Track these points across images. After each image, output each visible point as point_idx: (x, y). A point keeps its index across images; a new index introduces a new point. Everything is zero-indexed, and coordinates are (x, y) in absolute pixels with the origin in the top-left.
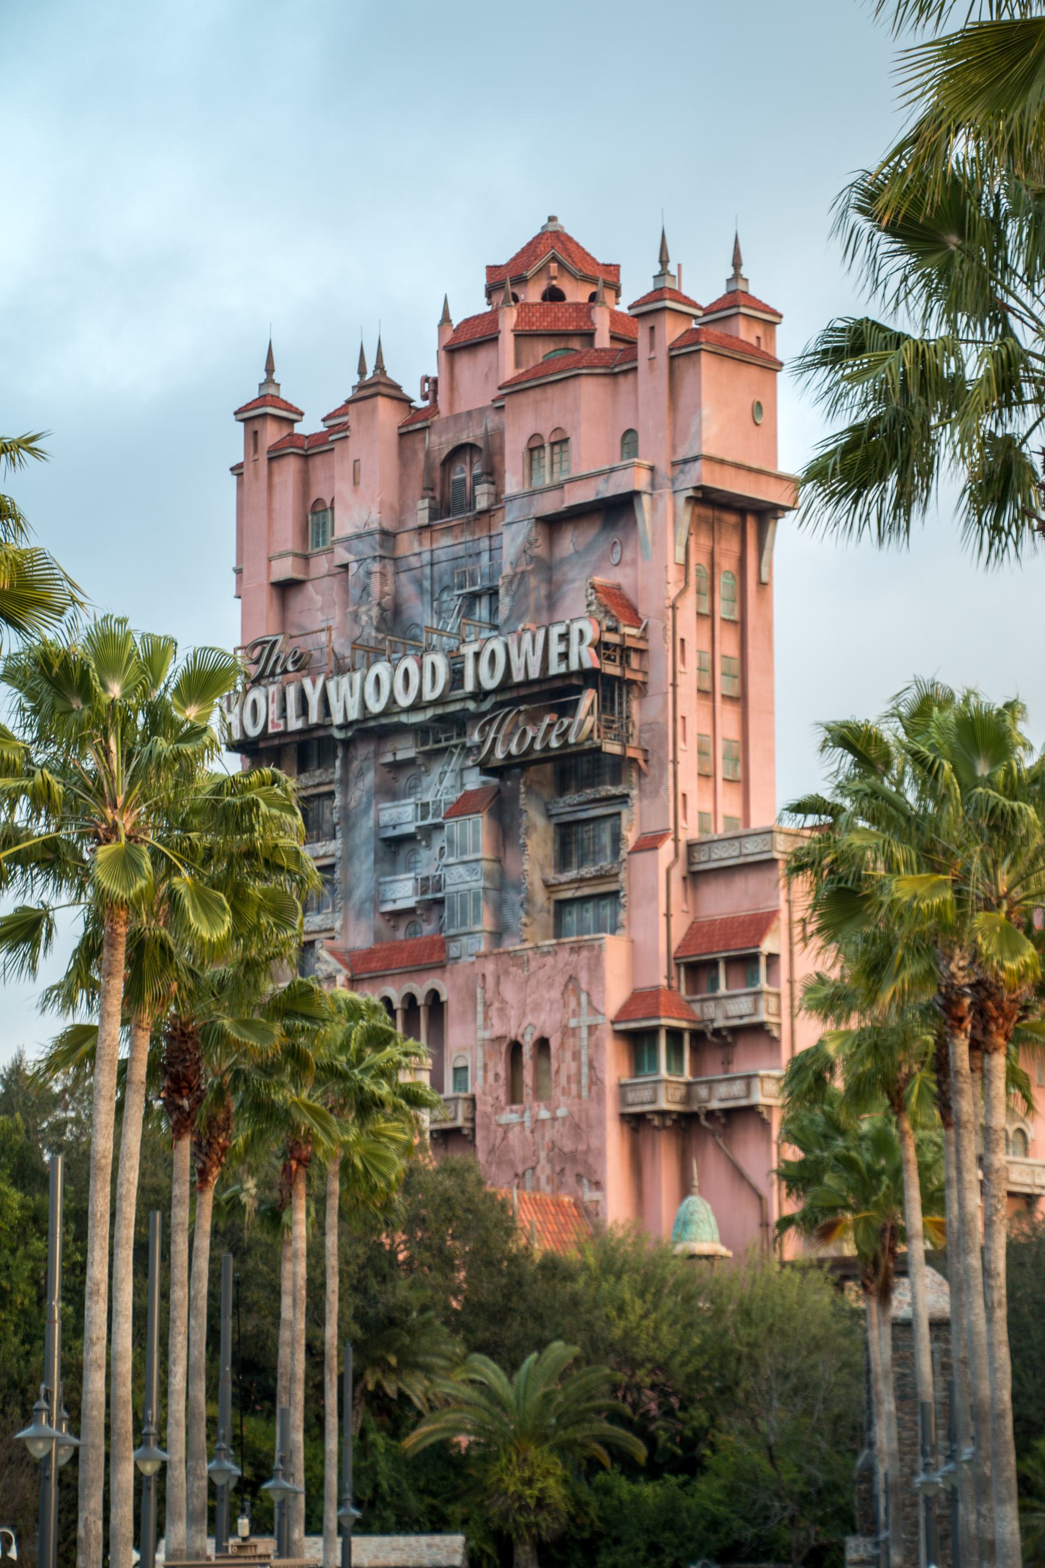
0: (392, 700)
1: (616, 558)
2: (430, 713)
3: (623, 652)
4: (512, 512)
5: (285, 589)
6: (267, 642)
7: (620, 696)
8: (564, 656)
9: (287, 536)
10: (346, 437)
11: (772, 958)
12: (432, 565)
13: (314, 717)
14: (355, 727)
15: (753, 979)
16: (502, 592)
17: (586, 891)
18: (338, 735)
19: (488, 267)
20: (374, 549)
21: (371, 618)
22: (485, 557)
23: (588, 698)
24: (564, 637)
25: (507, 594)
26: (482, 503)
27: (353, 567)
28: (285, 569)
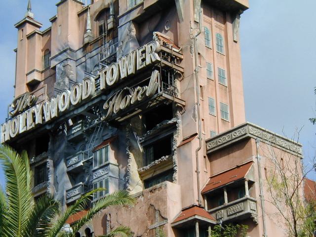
0: (70, 103)
2: (86, 107)
3: (173, 59)
4: (122, 22)
5: (33, 85)
7: (171, 77)
8: (144, 60)
11: (251, 184)
13: (38, 120)
14: (55, 122)
15: (243, 193)
17: (158, 172)
18: (48, 128)
23: (156, 74)
24: (144, 52)
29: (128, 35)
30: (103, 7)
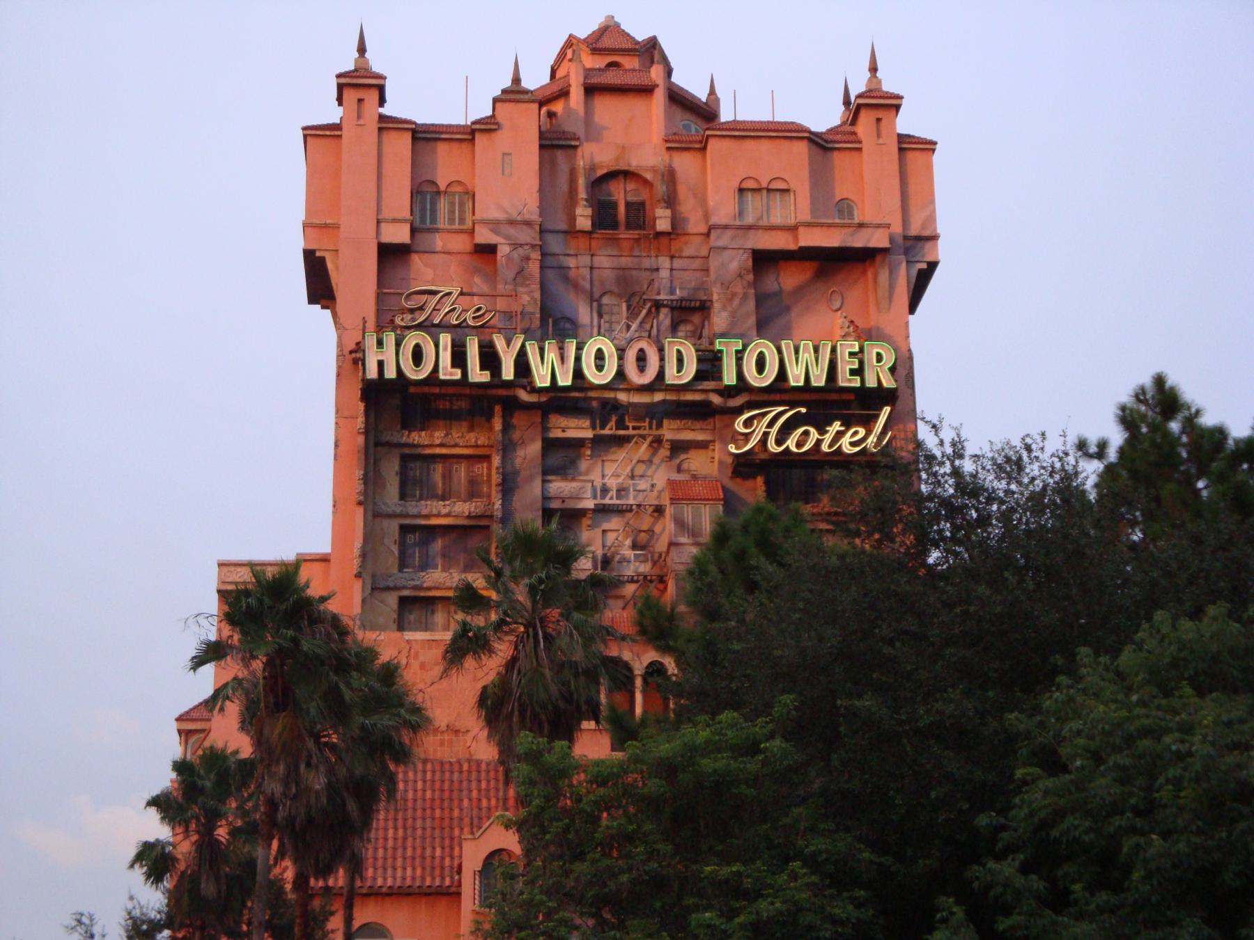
1: (837, 305)
6: (434, 293)
9: (399, 200)
10: (495, 130)
12: (591, 268)
16: (717, 306)
19: (571, 36)
20: (534, 239)
21: (533, 298)
22: (664, 274)
25: (724, 308)
26: (663, 225)
27: (503, 250)
28: (399, 234)
29: (740, 276)
30: (622, 166)
